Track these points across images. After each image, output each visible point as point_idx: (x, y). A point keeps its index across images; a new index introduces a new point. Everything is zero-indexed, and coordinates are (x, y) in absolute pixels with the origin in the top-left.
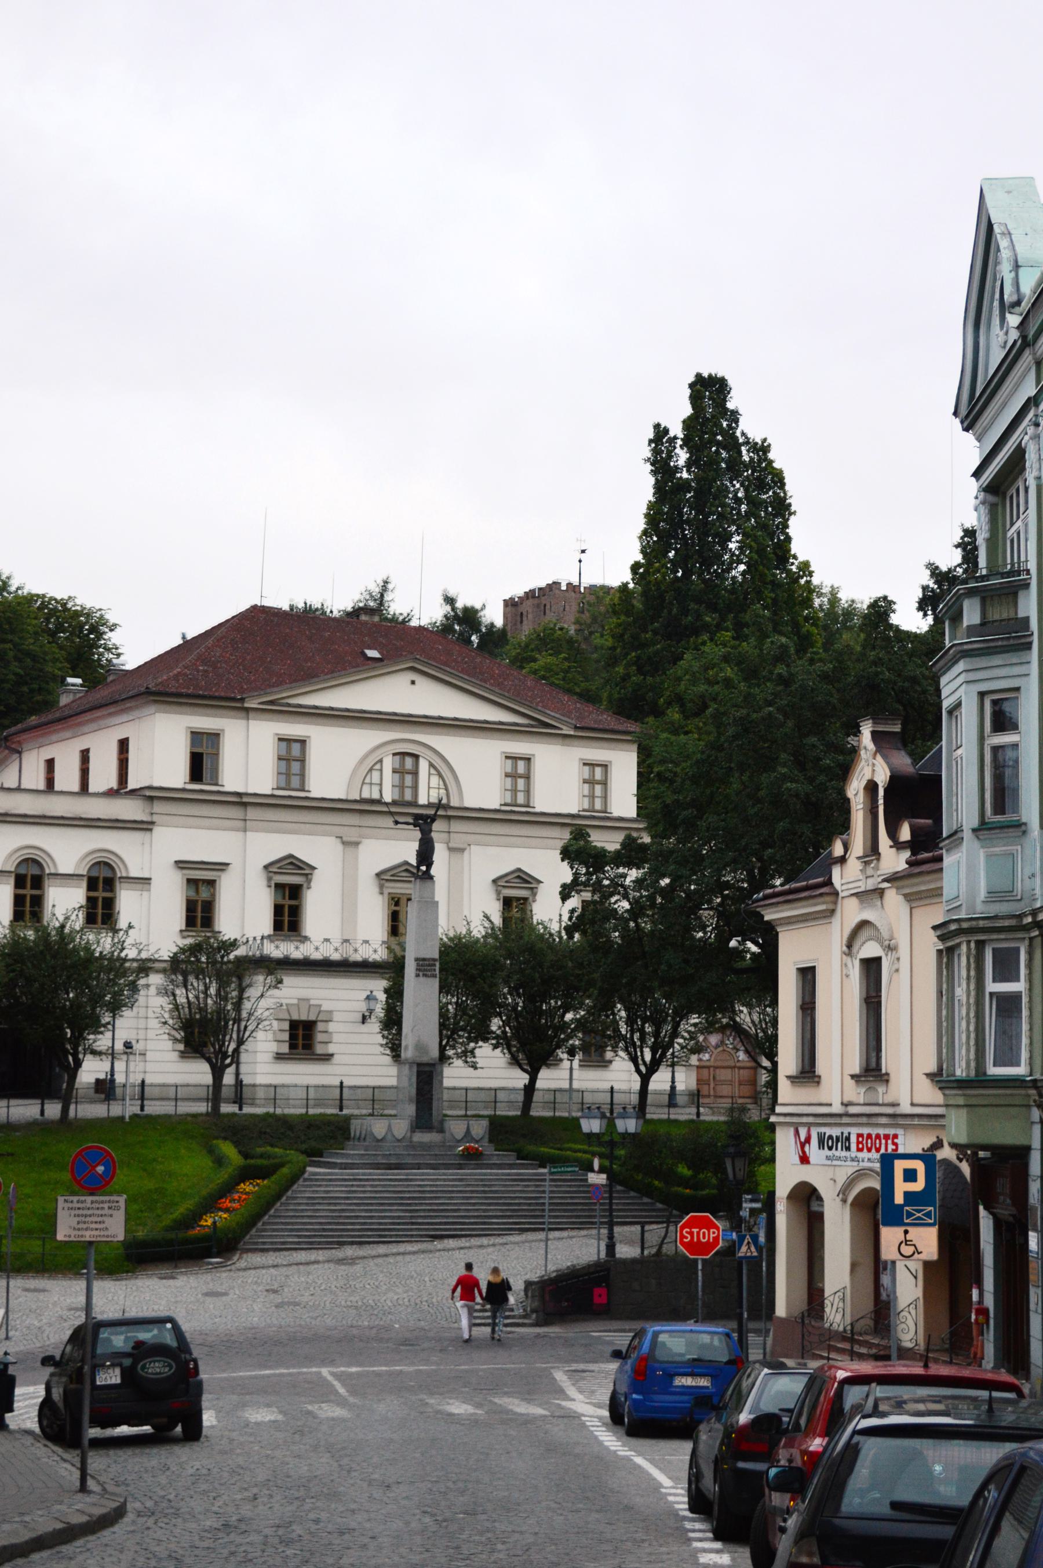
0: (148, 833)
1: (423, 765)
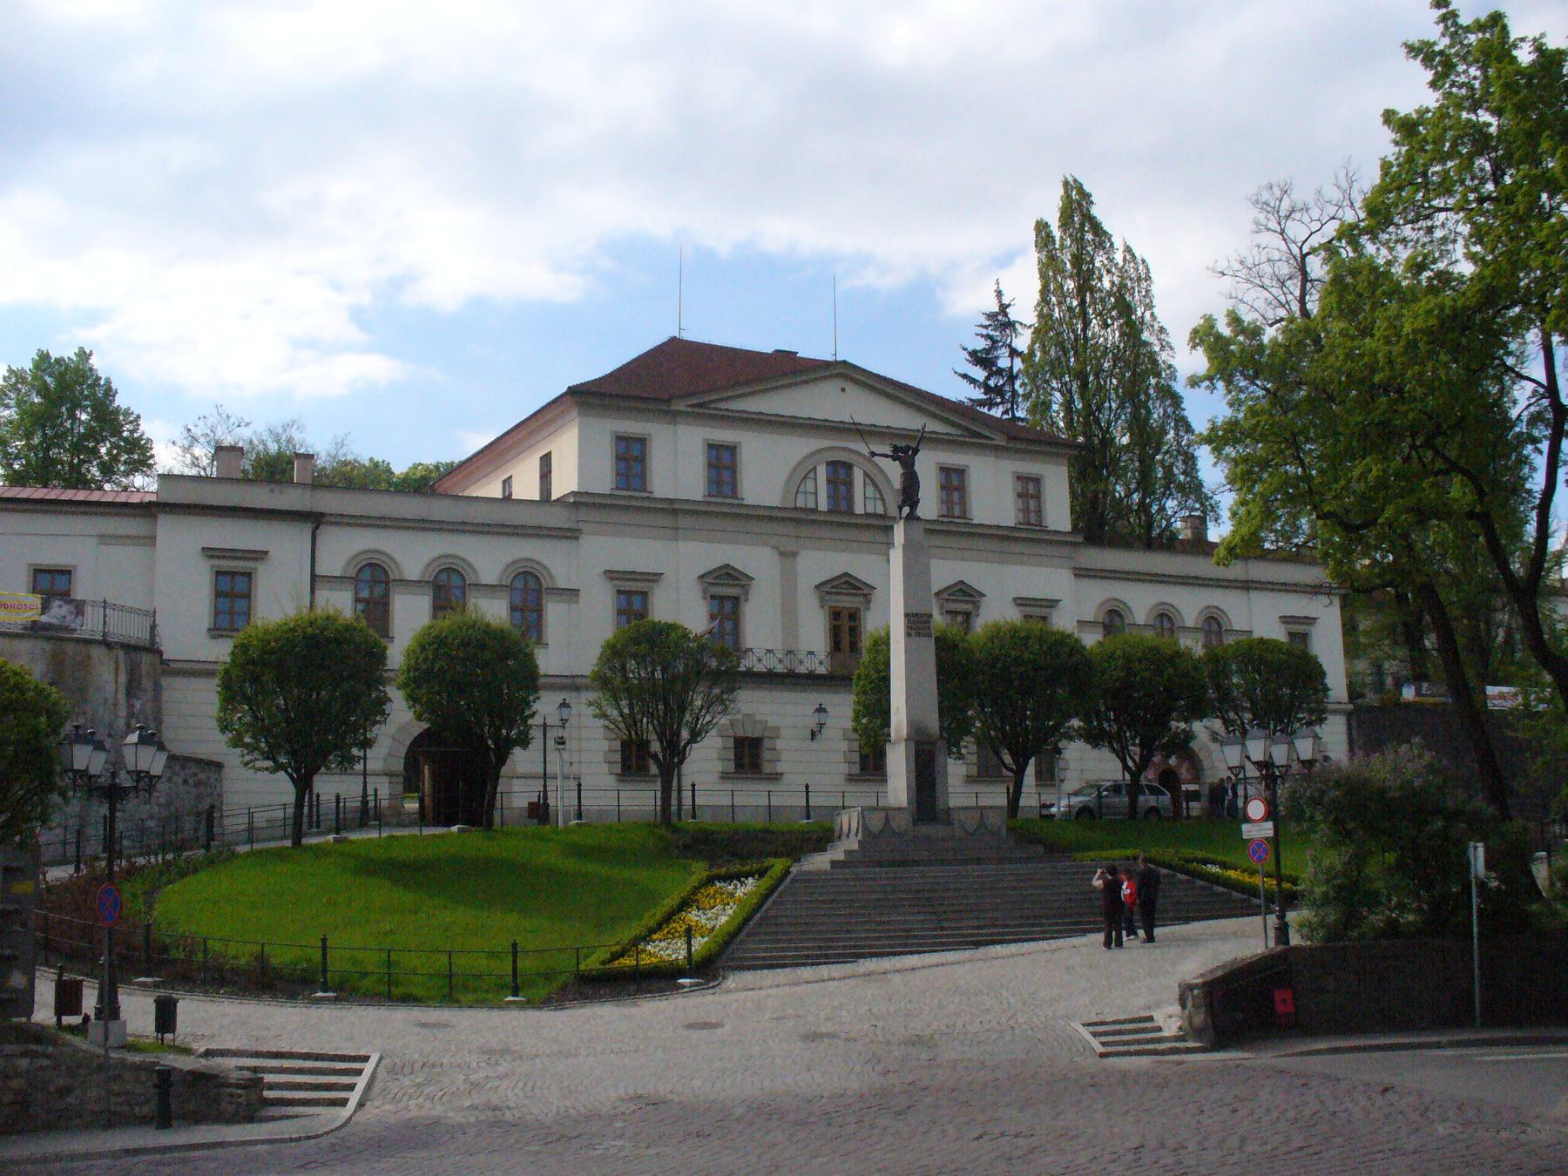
1: (858, 476)
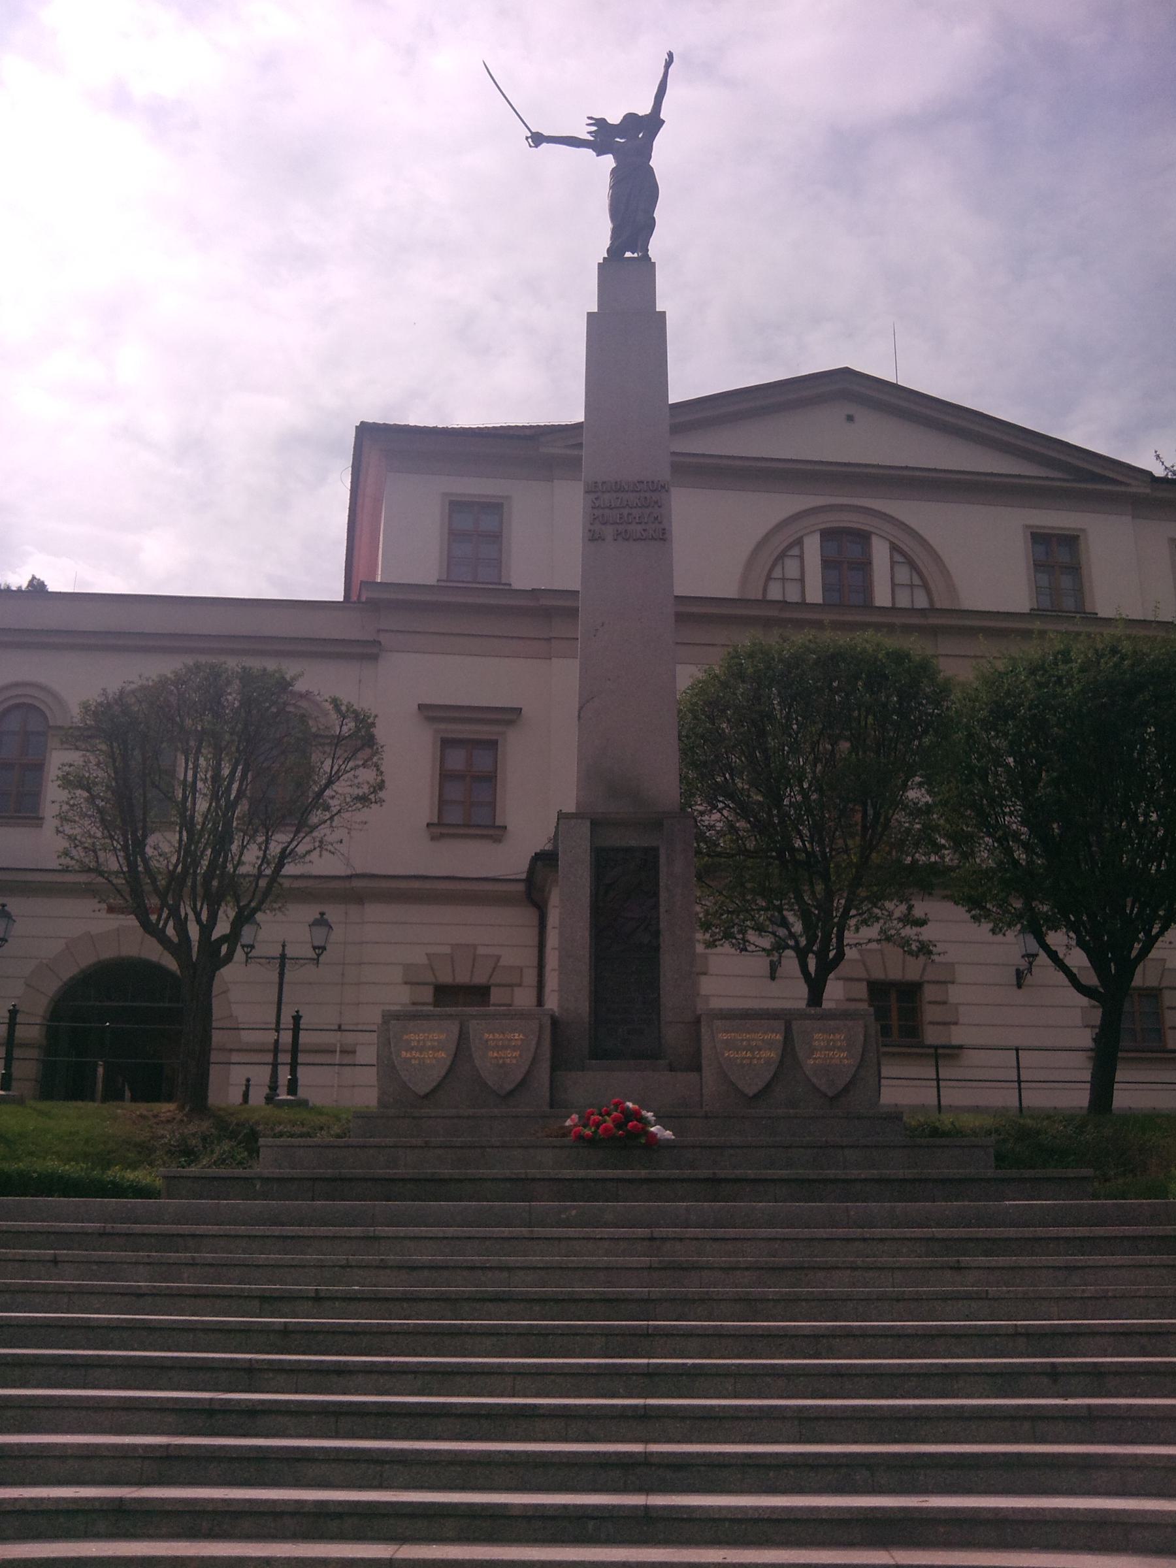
1: (880, 553)
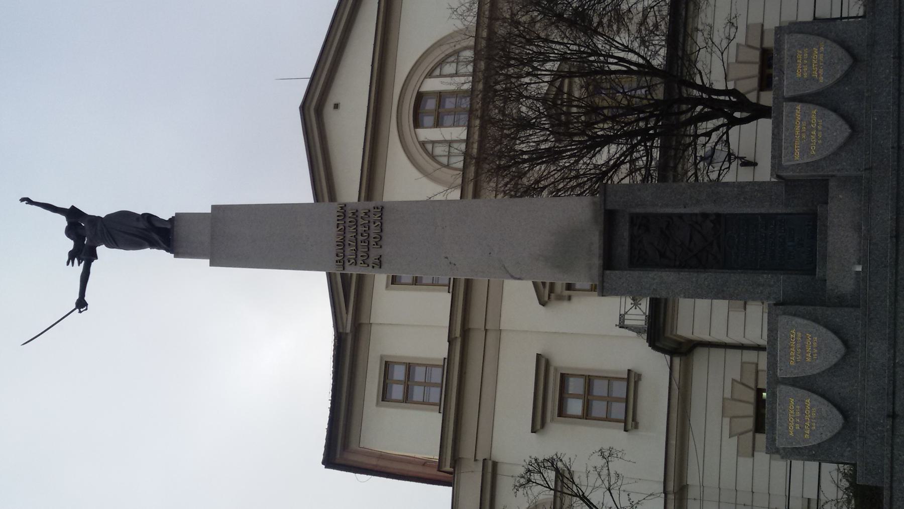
0: (501, 470)
1: (433, 85)
